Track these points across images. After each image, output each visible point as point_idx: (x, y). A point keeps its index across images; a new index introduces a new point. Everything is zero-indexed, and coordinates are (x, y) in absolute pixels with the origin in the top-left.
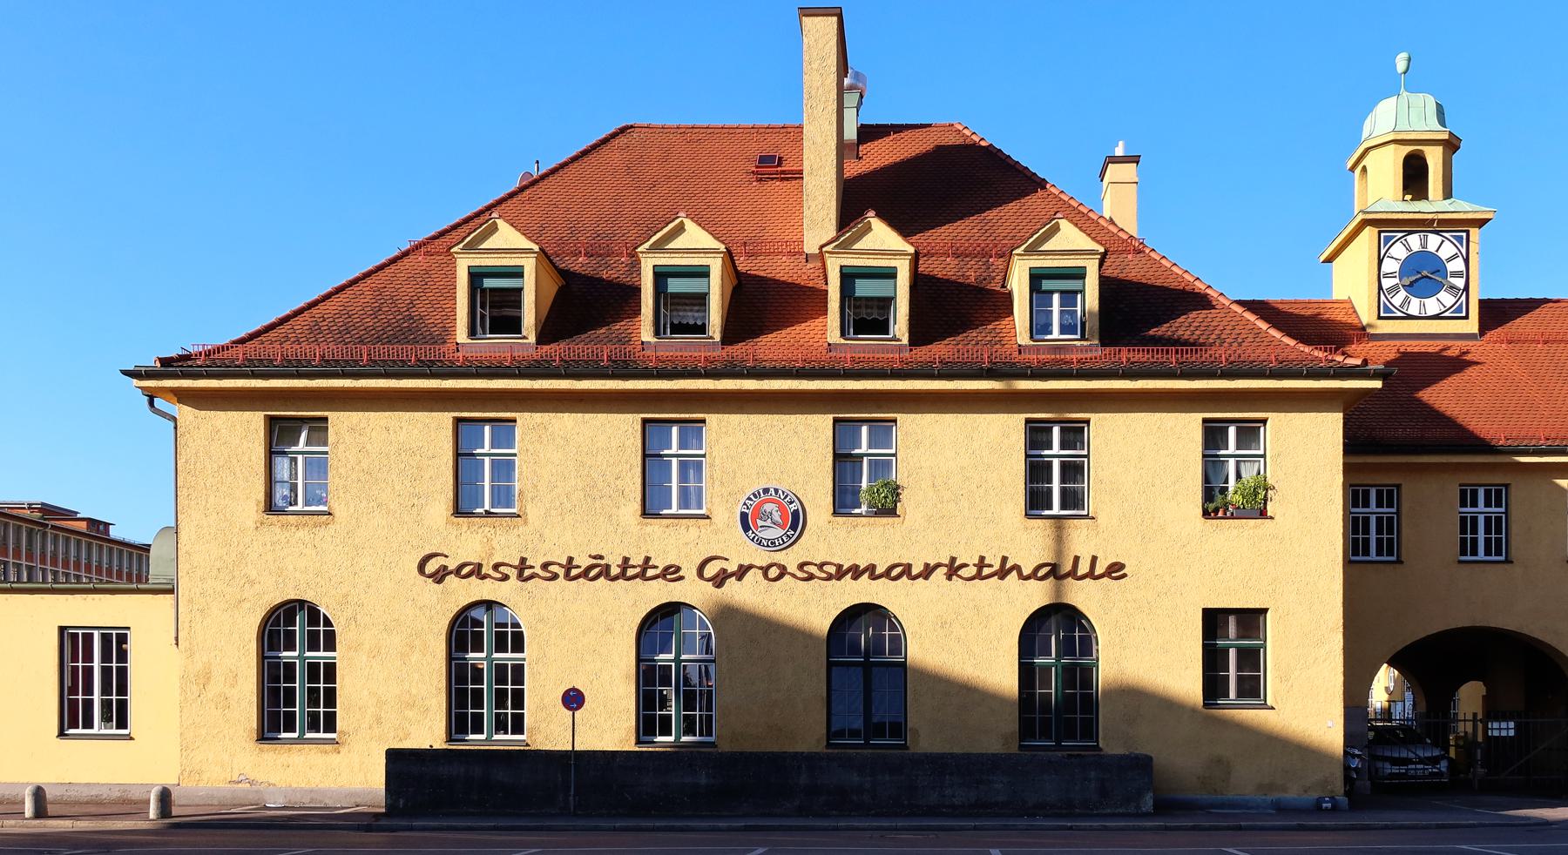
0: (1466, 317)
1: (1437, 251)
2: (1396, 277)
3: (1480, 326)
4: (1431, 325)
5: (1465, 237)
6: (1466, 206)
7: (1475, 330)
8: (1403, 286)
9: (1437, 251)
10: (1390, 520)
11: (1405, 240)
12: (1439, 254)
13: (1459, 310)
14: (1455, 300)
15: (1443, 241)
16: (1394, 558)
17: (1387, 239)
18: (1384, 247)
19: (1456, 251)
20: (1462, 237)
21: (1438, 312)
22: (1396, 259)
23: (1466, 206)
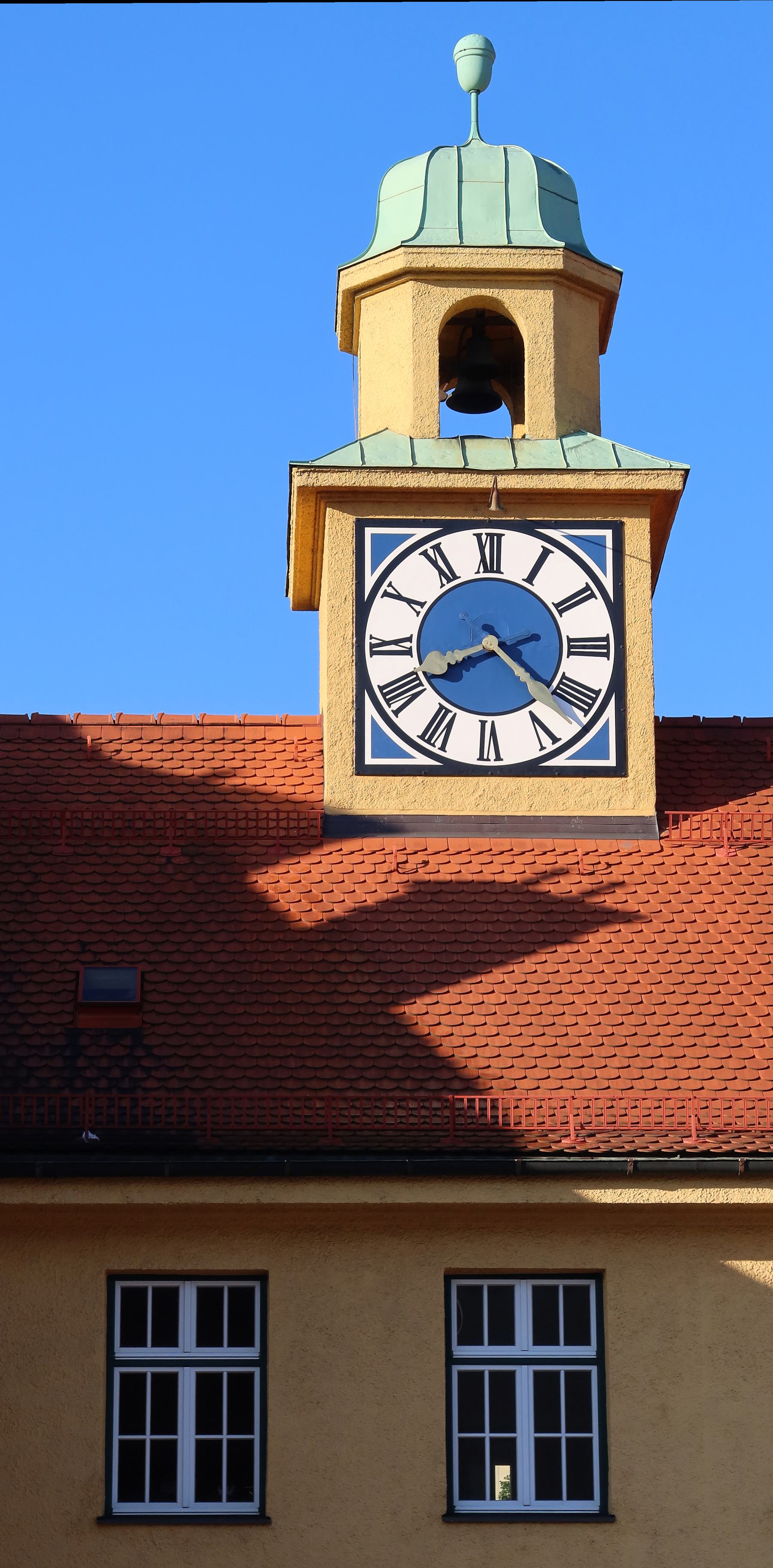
0: (620, 770)
1: (530, 579)
2: (409, 652)
3: (658, 795)
5: (609, 543)
6: (633, 458)
7: (647, 808)
8: (430, 677)
9: (530, 579)
10: (578, 1382)
11: (437, 548)
12: (538, 587)
13: (597, 748)
15: (546, 553)
16: (592, 1506)
17: (383, 545)
18: (373, 572)
19: (583, 579)
20: (600, 543)
21: (534, 753)
22: (410, 602)
23: (633, 458)
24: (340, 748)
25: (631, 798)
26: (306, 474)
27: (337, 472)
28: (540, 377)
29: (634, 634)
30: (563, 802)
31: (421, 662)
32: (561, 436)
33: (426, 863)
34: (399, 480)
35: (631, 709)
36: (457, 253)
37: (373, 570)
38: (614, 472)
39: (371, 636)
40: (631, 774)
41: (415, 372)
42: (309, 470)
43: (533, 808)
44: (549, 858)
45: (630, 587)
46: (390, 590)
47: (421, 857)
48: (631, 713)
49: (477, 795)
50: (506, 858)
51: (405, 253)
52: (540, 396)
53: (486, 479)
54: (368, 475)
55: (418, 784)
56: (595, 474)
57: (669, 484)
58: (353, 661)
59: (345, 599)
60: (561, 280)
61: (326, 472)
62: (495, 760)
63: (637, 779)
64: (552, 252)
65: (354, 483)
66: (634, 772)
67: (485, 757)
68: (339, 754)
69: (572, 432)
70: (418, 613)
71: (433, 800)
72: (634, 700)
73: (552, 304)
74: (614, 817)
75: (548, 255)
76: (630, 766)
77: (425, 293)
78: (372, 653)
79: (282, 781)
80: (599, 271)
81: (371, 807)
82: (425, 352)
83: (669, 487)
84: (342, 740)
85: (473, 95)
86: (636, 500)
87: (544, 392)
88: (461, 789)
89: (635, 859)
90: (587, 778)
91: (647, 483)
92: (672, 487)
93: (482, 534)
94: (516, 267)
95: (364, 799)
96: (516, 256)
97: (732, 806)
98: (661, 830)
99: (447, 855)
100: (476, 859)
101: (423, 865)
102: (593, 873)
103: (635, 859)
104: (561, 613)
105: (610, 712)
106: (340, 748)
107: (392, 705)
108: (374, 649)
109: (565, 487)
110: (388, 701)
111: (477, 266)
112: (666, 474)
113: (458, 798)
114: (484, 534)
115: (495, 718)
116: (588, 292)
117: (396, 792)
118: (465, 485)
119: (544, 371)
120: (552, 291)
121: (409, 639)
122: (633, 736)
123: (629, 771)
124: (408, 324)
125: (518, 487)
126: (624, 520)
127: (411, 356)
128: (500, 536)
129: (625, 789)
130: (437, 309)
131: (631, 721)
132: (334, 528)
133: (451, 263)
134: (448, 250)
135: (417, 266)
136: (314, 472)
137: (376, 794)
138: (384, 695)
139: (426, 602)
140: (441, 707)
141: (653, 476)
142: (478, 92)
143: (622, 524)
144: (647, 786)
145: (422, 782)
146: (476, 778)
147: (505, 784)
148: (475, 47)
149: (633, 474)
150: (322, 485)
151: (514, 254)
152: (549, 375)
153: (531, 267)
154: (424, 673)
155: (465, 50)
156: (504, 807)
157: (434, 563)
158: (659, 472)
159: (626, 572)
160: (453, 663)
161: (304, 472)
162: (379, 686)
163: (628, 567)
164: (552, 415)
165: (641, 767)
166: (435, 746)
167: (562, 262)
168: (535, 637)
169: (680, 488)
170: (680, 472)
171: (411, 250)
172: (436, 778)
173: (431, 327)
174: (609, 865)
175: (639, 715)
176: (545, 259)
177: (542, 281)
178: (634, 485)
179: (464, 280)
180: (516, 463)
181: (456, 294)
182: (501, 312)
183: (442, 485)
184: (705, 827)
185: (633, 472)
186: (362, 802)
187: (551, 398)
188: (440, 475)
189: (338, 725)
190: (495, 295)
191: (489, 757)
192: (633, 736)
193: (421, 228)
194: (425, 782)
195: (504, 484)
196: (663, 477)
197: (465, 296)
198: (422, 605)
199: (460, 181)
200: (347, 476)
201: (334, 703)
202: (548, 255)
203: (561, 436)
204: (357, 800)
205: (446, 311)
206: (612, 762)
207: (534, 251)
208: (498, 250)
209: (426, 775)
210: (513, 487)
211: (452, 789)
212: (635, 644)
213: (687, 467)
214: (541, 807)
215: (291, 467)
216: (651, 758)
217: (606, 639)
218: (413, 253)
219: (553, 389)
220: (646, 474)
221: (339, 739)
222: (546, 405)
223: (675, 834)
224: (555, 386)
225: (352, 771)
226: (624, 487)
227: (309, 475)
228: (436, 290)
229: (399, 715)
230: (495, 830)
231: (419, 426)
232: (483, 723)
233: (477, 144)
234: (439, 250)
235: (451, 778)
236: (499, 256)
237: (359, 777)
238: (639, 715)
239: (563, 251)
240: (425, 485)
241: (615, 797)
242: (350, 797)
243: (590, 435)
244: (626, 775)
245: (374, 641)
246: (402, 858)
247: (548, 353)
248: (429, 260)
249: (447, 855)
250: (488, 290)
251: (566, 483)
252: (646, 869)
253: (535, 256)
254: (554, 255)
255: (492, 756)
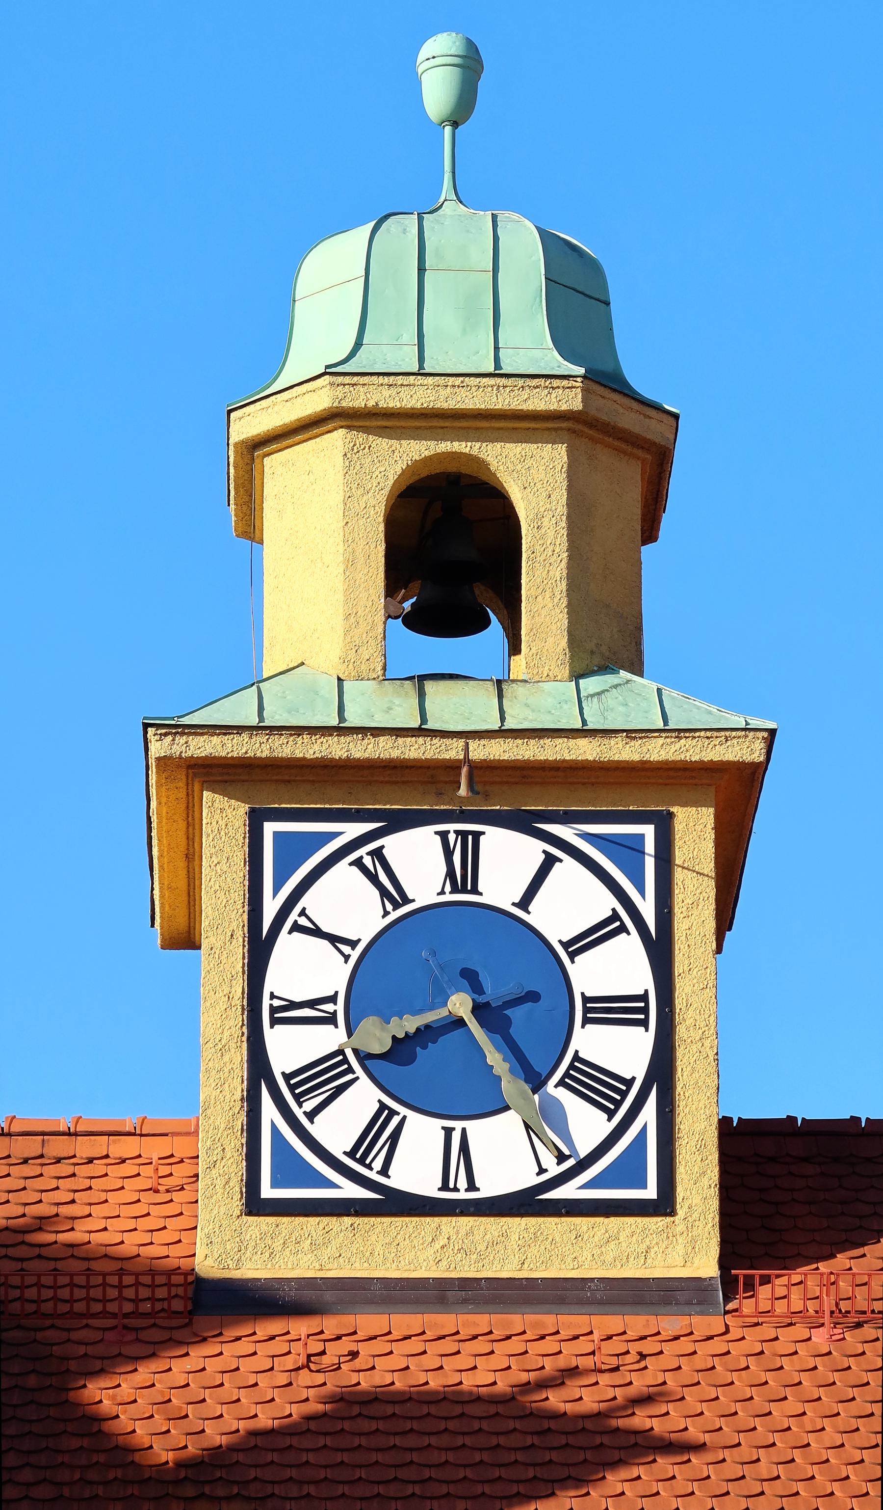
1: (524, 903)
2: (331, 1020)
3: (724, 1243)
4: (505, 1235)
5: (650, 846)
8: (363, 1057)
9: (524, 903)
11: (378, 854)
14: (609, 1127)
15: (549, 862)
18: (276, 891)
19: (607, 903)
20: (635, 845)
22: (334, 939)
24: (221, 1172)
25: (680, 1249)
26: (170, 738)
27: (219, 735)
28: (545, 582)
29: (688, 990)
30: (573, 1256)
31: (350, 1034)
32: (577, 676)
33: (354, 1355)
34: (316, 747)
35: (681, 1108)
36: (414, 385)
37: (276, 891)
38: (657, 734)
39: (272, 993)
40: (681, 1212)
41: (348, 573)
42: (174, 731)
43: (526, 1266)
44: (549, 1345)
45: (682, 916)
46: (303, 921)
47: (346, 1345)
48: (682, 1114)
49: (437, 1246)
50: (482, 1346)
51: (332, 384)
52: (544, 612)
53: (455, 745)
54: (268, 739)
55: (344, 1228)
56: (627, 737)
57: (745, 752)
58: (243, 1034)
59: (232, 935)
60: (579, 427)
61: (202, 734)
62: (466, 1190)
63: (689, 1218)
64: (565, 383)
65: (246, 753)
66: (686, 1209)
67: (451, 1186)
68: (220, 1182)
69: (596, 668)
70: (347, 958)
71: (368, 1254)
72: (687, 1095)
73: (565, 466)
74: (653, 1279)
75: (558, 387)
76: (679, 1199)
77: (364, 449)
78: (274, 1022)
79: (131, 1224)
80: (640, 413)
81: (269, 1266)
82: (363, 542)
83: (744, 758)
84: (225, 1160)
85: (448, 130)
86: (693, 777)
87: (550, 605)
88: (413, 1235)
89: (685, 1345)
90: (612, 1219)
91: (708, 751)
92: (748, 758)
93: (449, 832)
94: (507, 408)
95: (259, 1253)
96: (508, 389)
97: (842, 1260)
98: (727, 1299)
99: (388, 1341)
100: (434, 1348)
101: (350, 1357)
102: (616, 1369)
103: (685, 1345)
104: (572, 956)
105: (649, 1113)
106: (221, 1172)
107: (304, 1104)
108: (276, 1015)
109: (580, 758)
110: (298, 1098)
111: (445, 406)
112: (739, 737)
113: (407, 1250)
114: (452, 832)
115: (467, 1124)
116: (623, 446)
117: (309, 1241)
118: (421, 755)
119: (551, 573)
120: (566, 445)
121: (333, 999)
122: (684, 1151)
123: (678, 1206)
124: (336, 497)
125: (506, 758)
126: (674, 809)
127: (341, 548)
128: (477, 835)
129: (670, 1235)
130: (383, 474)
131: (681, 1127)
132: (214, 823)
133: (405, 401)
134: (400, 380)
135: (351, 405)
136: (182, 734)
137: (277, 1245)
138: (292, 1088)
139: (359, 940)
140: (383, 1106)
141: (719, 739)
142: (455, 124)
143: (671, 815)
144: (706, 1229)
145: (352, 1225)
146: (436, 1219)
147: (482, 1228)
148: (449, 53)
149: (686, 737)
150: (195, 756)
151: (504, 387)
152: (558, 579)
153: (531, 408)
154: (356, 1051)
155: (434, 57)
156: (481, 1264)
157: (373, 878)
158: (727, 733)
159: (676, 892)
160: (401, 1035)
161: (166, 735)
162: (283, 1074)
163: (680, 883)
164: (564, 642)
165: (696, 1200)
166: (371, 1169)
167: (580, 400)
168: (532, 997)
169: (762, 759)
170: (761, 735)
171: (340, 379)
172: (374, 1219)
173: (372, 502)
174: (642, 1356)
175: (695, 1119)
176: (553, 395)
177: (548, 429)
178: (688, 754)
179: (426, 428)
180: (503, 719)
181: (412, 449)
182: (484, 478)
183: (385, 755)
184: (796, 1295)
185: (687, 735)
186: (255, 1257)
187: (561, 615)
188: (382, 738)
189: (219, 1135)
190: (475, 452)
191: (458, 1186)
192: (684, 1151)
193: (358, 345)
194: (356, 1225)
195: (482, 754)
196: (735, 741)
197: (427, 453)
198: (353, 944)
199: (422, 270)
200: (235, 740)
201: (213, 1102)
202: (558, 387)
203: (577, 676)
204: (248, 1254)
205: (396, 477)
206: (650, 1192)
207: (535, 382)
208: (478, 380)
209: (357, 1214)
210: (497, 758)
211: (399, 1237)
212: (688, 1005)
213: (771, 725)
214: (538, 1264)
215: (146, 726)
216: (713, 1185)
217: (644, 997)
218: (344, 385)
219: (565, 602)
220: (708, 738)
221: (219, 1158)
222: (554, 627)
223: (748, 1307)
224: (568, 596)
225: (240, 1208)
226: (673, 758)
227: (173, 740)
228: (382, 444)
229: (315, 1120)
230: (465, 1301)
231: (352, 661)
232: (448, 1131)
233: (451, 209)
234: (386, 380)
235: (397, 1219)
236: (481, 390)
237: (251, 1218)
238: (695, 1119)
239: (582, 382)
240: (357, 755)
241: (656, 1248)
242: (236, 1249)
243: (624, 674)
244: (672, 1213)
245: (276, 1003)
246: (318, 1347)
247: (557, 543)
248: (369, 396)
249: (388, 1341)
250: (464, 444)
251: (582, 751)
252: (700, 1362)
253: (538, 390)
254: (568, 388)
255: (463, 1183)
